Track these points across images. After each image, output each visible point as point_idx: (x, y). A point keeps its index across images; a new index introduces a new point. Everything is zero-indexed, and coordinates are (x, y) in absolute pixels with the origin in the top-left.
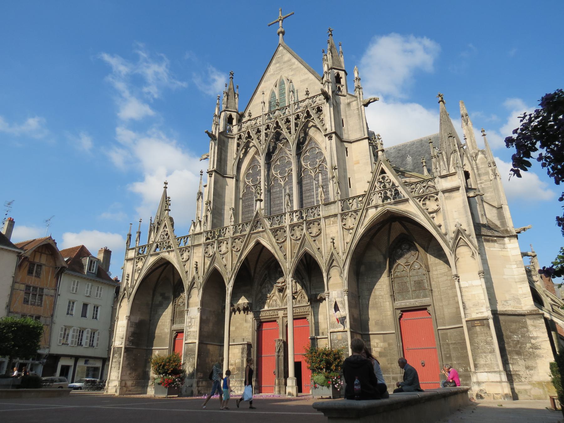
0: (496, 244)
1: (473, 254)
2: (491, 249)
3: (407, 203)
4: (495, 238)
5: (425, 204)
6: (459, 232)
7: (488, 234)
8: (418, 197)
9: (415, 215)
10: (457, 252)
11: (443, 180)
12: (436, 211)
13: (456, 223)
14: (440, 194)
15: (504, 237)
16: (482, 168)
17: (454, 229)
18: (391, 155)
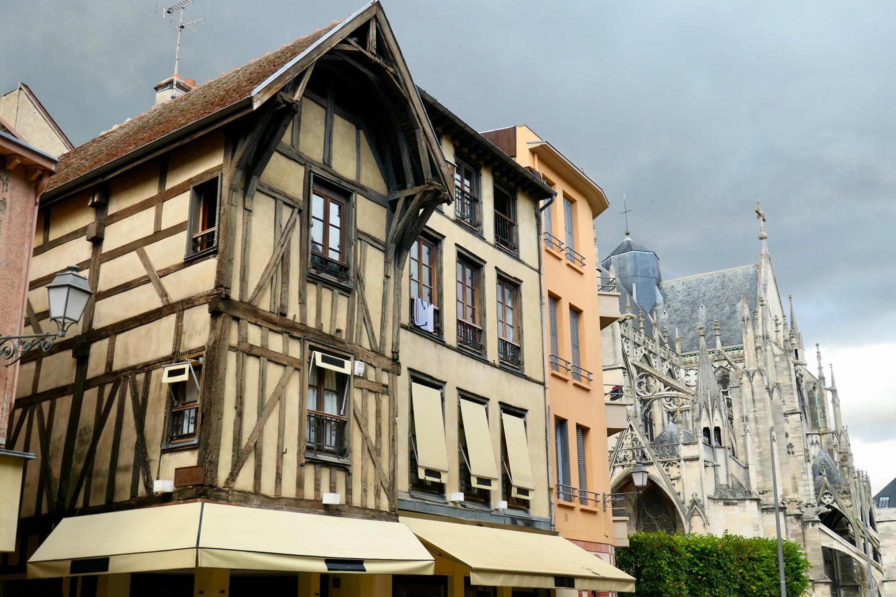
0: (736, 507)
1: (704, 524)
2: (730, 513)
3: (652, 467)
4: (736, 501)
5: (667, 470)
6: (694, 502)
7: (728, 498)
8: (662, 462)
9: (658, 480)
10: (692, 520)
11: (686, 447)
12: (678, 479)
13: (692, 493)
14: (682, 462)
15: (745, 500)
16: (757, 392)
17: (691, 498)
18: (678, 296)
